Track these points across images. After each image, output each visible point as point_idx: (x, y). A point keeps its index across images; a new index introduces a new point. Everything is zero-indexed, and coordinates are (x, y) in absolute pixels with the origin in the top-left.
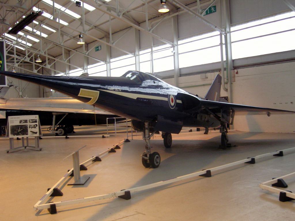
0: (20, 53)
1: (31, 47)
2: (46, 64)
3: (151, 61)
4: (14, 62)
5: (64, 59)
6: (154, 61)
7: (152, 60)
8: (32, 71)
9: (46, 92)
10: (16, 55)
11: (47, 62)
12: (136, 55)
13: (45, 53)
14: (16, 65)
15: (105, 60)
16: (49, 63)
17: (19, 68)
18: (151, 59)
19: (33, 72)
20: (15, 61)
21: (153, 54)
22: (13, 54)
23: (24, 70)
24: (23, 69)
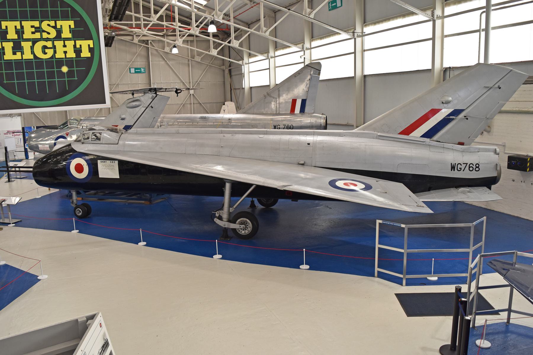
0: (186, 19)
1: (205, 6)
2: (230, 41)
3: (483, 34)
4: (175, 35)
5: (264, 29)
6: (493, 33)
7: (487, 30)
8: (209, 52)
9: (235, 89)
10: (180, 21)
11: (233, 35)
12: (435, 17)
13: (227, 15)
14: (180, 42)
15: (349, 28)
16: (237, 38)
17: (188, 48)
18: (483, 27)
19: (210, 53)
20: (178, 33)
21: (493, 14)
22: (174, 20)
23: (197, 51)
24: (189, 47)
